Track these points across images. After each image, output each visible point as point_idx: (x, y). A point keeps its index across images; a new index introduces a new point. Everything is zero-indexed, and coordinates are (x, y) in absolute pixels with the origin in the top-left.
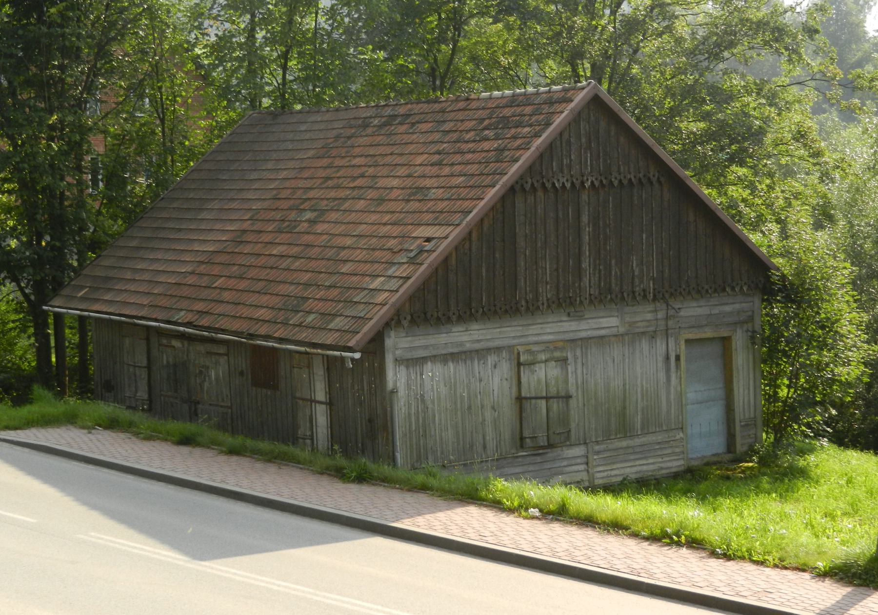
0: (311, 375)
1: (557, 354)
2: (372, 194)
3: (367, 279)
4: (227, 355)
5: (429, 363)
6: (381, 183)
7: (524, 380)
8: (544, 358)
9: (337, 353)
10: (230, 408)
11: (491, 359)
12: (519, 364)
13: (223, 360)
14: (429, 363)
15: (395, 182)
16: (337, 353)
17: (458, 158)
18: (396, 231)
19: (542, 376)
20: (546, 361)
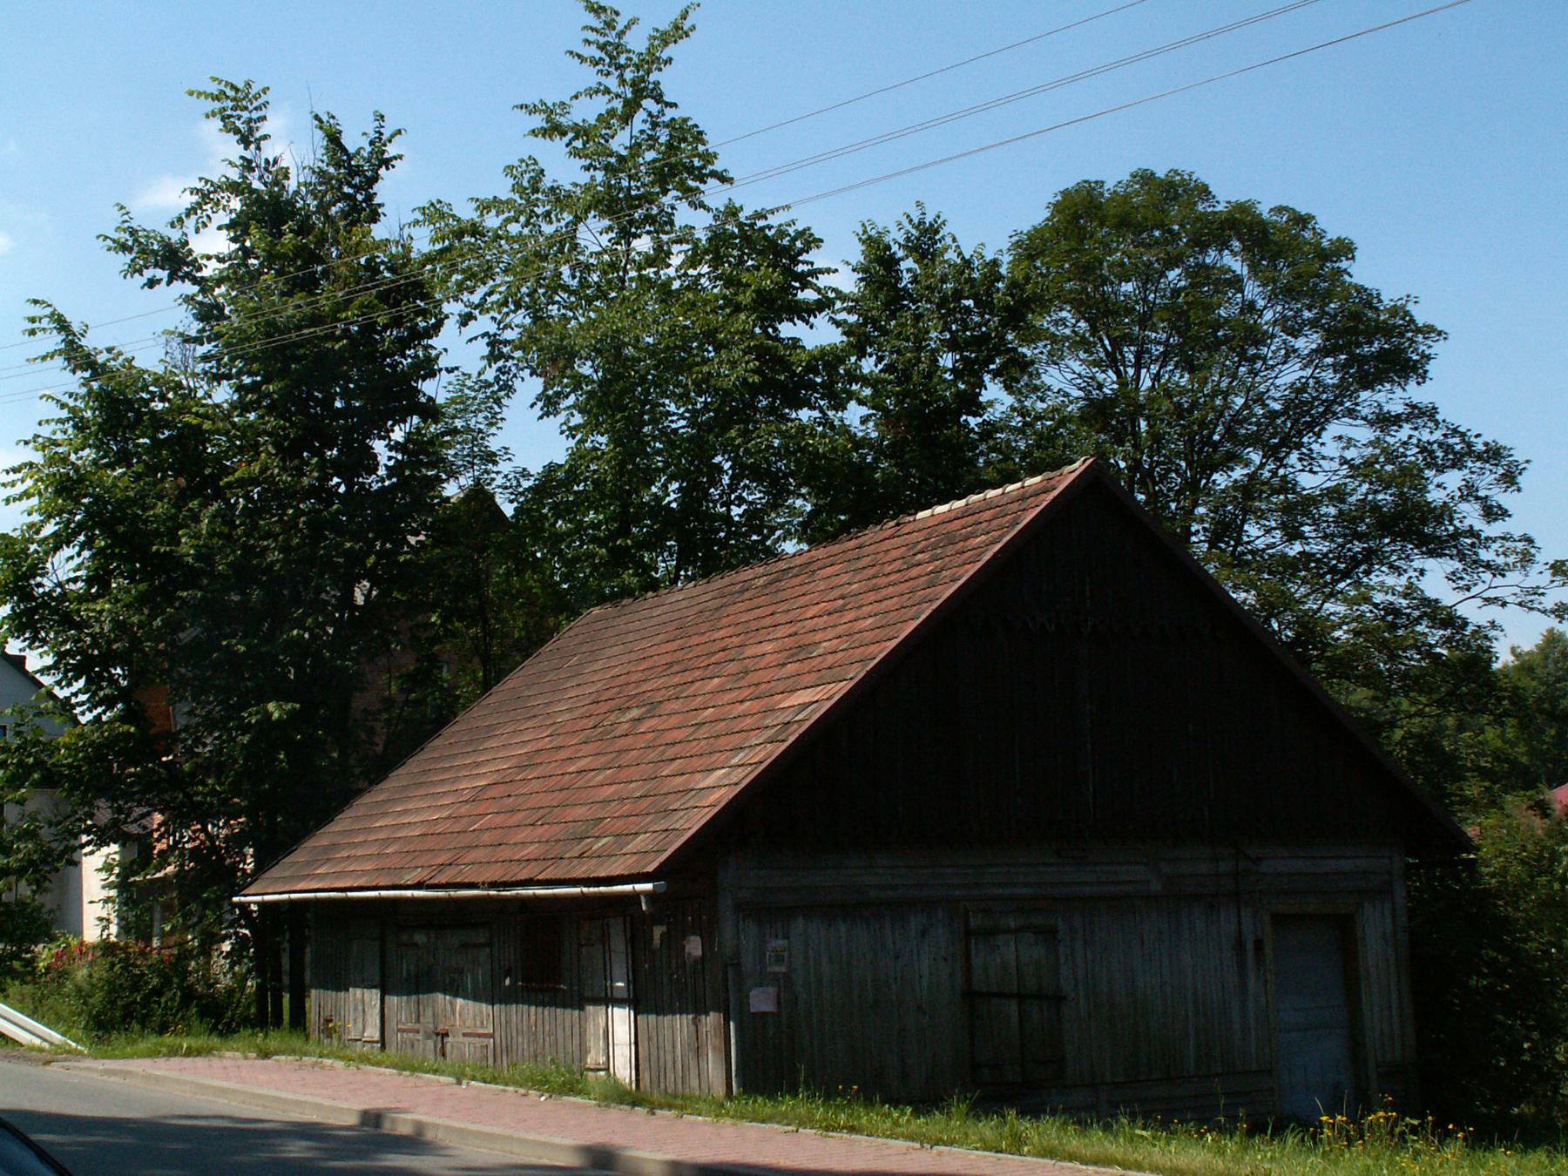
0: (607, 952)
1: (1038, 920)
2: (732, 667)
3: (698, 776)
4: (490, 945)
5: (801, 919)
6: (749, 652)
7: (976, 962)
8: (1012, 924)
9: (628, 888)
10: (492, 1036)
11: (915, 923)
12: (968, 933)
13: (483, 954)
14: (801, 919)
15: (769, 647)
16: (628, 888)
17: (872, 597)
18: (756, 705)
19: (1010, 956)
20: (1016, 931)
